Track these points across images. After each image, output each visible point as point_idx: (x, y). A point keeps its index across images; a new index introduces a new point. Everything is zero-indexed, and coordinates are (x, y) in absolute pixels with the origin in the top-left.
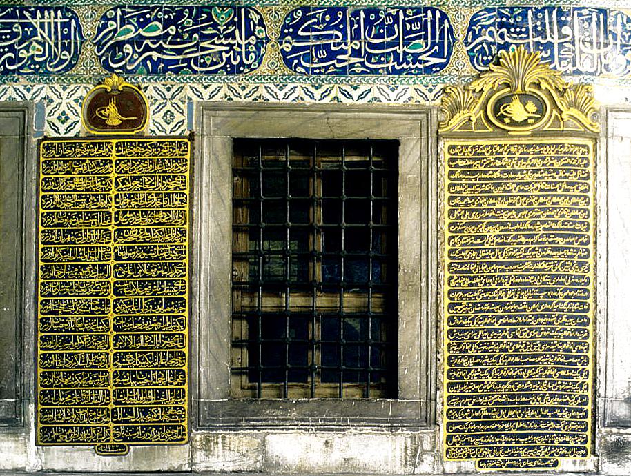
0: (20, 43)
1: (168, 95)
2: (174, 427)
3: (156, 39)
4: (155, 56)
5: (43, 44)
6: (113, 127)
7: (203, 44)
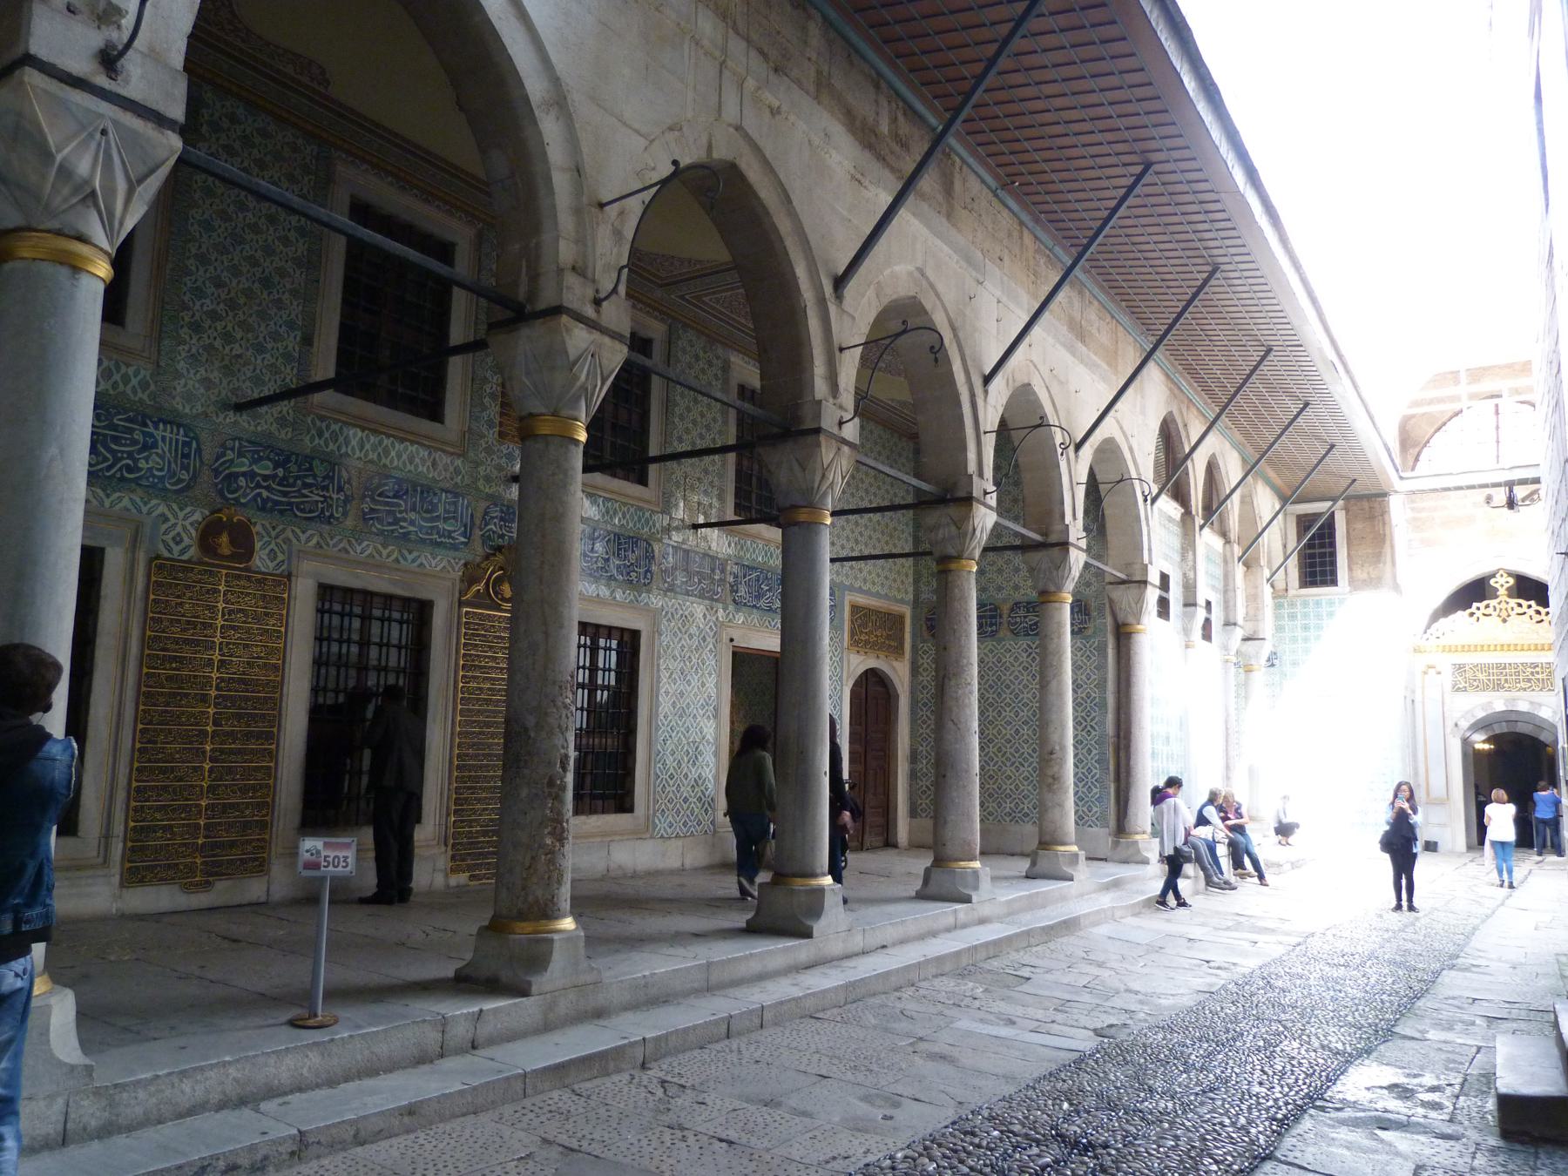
1: (273, 534)
2: (256, 859)
3: (265, 478)
4: (265, 494)
6: (223, 557)
7: (305, 491)
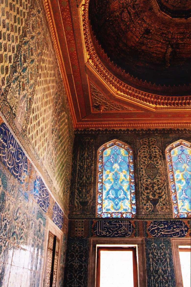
0: (118, 229)
3: (162, 229)
4: (163, 233)
5: (124, 230)
7: (174, 230)
